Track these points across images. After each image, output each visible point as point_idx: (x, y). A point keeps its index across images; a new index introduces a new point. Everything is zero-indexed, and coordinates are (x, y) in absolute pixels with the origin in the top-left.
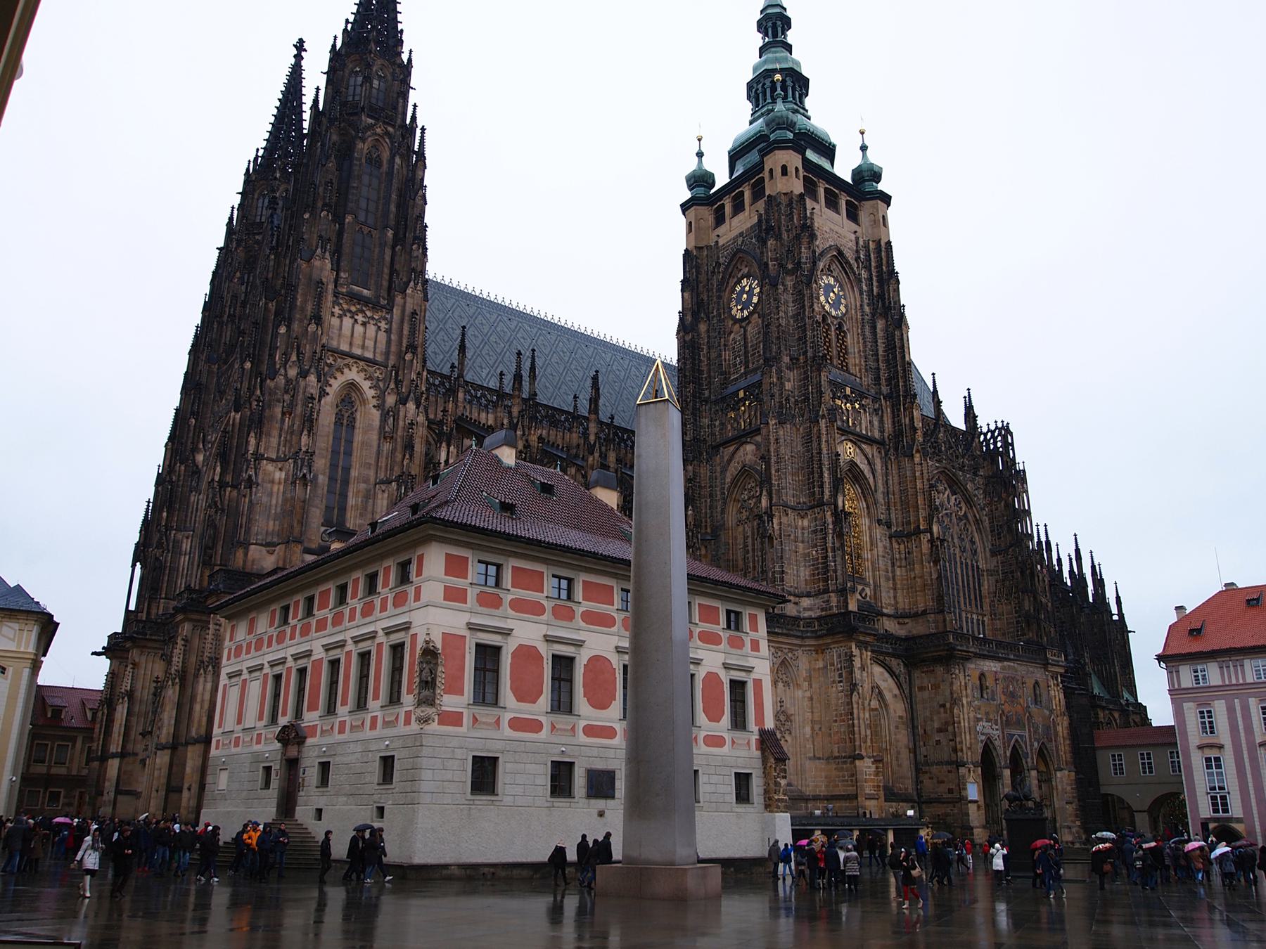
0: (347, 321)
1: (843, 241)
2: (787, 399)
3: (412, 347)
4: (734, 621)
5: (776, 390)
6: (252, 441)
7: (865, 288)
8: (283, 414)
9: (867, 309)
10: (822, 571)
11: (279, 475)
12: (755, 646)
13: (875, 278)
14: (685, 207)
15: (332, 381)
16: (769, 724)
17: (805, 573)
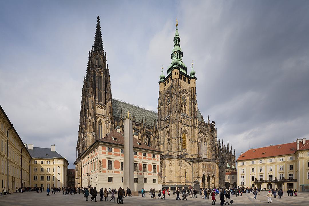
0: (99, 108)
1: (186, 88)
2: (174, 119)
3: (110, 113)
4: (154, 156)
5: (172, 118)
6: (85, 130)
7: (190, 97)
8: (90, 125)
9: (190, 101)
10: (178, 148)
11: (90, 136)
12: (158, 160)
13: (192, 95)
14: (160, 83)
15: (97, 119)
16: (160, 172)
17: (175, 149)
